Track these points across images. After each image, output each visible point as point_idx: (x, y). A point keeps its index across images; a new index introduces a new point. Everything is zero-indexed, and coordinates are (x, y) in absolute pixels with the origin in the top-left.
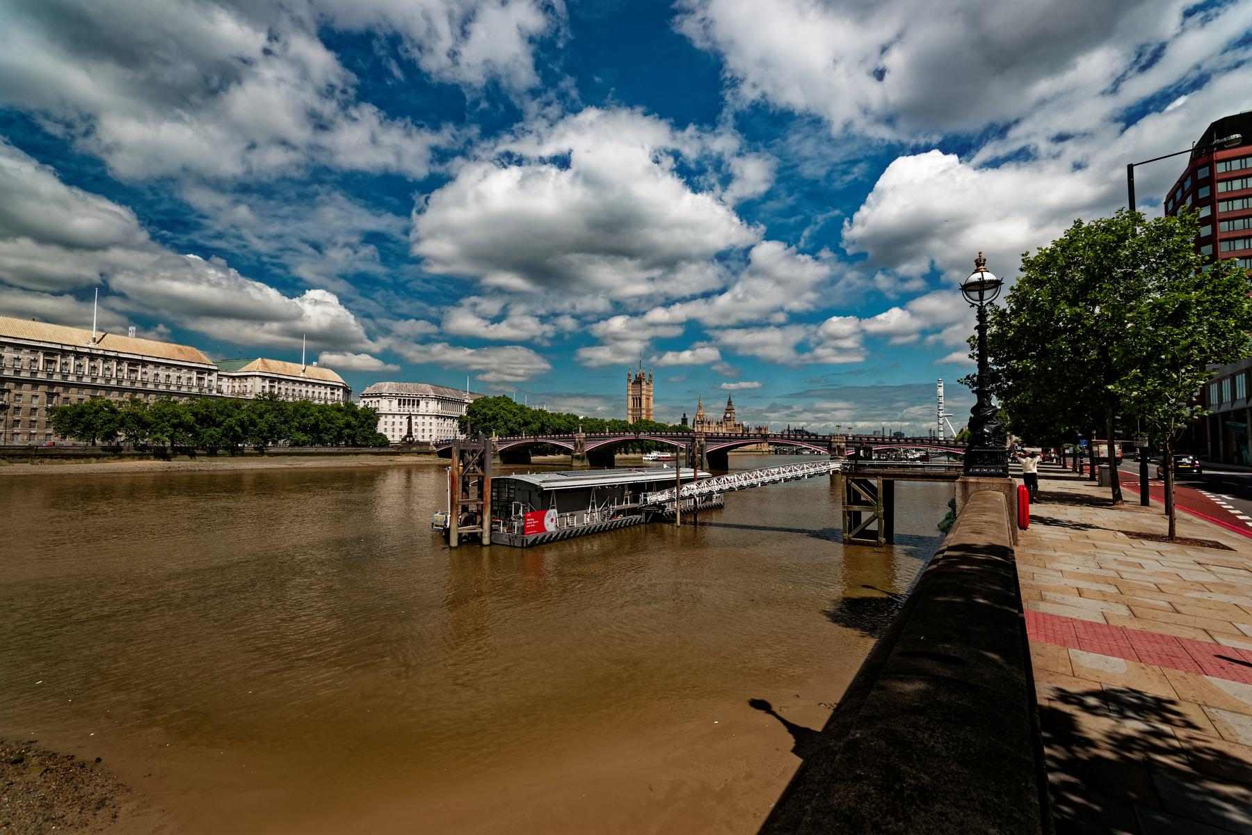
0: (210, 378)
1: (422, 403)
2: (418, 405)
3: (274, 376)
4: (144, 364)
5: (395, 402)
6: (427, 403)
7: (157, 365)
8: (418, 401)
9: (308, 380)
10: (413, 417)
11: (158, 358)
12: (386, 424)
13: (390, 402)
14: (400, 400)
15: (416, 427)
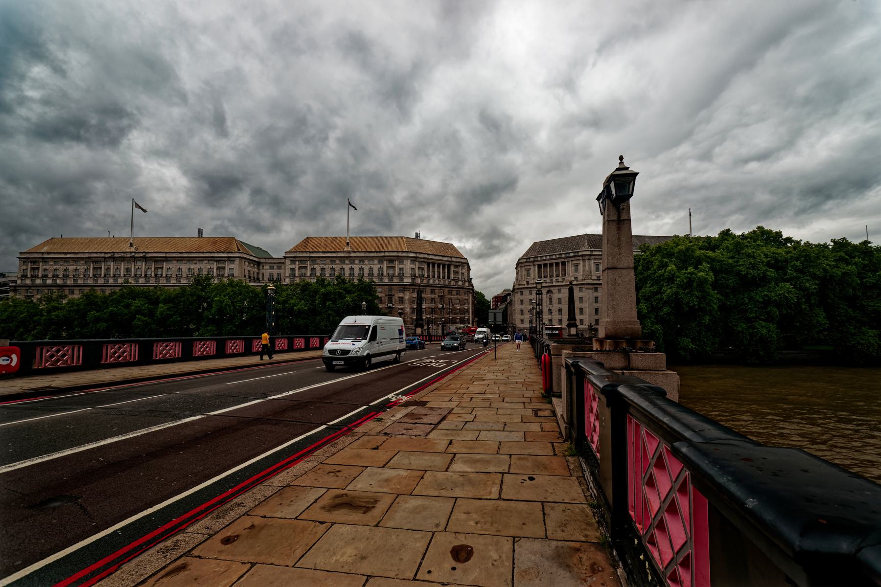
0: (231, 266)
1: (570, 268)
2: (564, 270)
3: (304, 254)
4: (166, 259)
5: (534, 271)
6: (576, 266)
7: (180, 260)
8: (564, 264)
9: (353, 254)
10: (555, 290)
11: (181, 253)
12: (522, 301)
13: (528, 270)
14: (539, 266)
15: (580, 306)
